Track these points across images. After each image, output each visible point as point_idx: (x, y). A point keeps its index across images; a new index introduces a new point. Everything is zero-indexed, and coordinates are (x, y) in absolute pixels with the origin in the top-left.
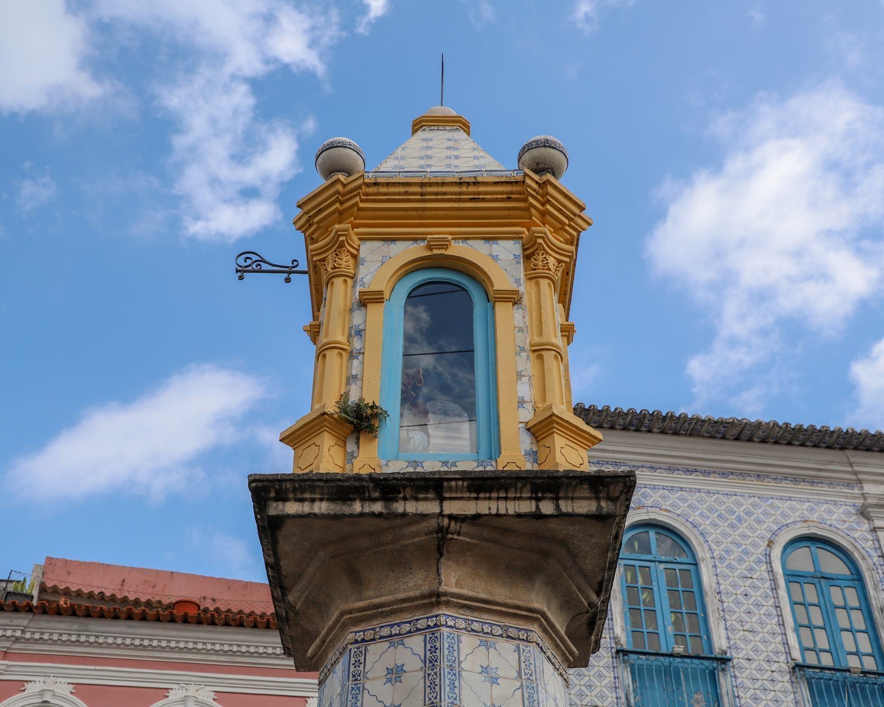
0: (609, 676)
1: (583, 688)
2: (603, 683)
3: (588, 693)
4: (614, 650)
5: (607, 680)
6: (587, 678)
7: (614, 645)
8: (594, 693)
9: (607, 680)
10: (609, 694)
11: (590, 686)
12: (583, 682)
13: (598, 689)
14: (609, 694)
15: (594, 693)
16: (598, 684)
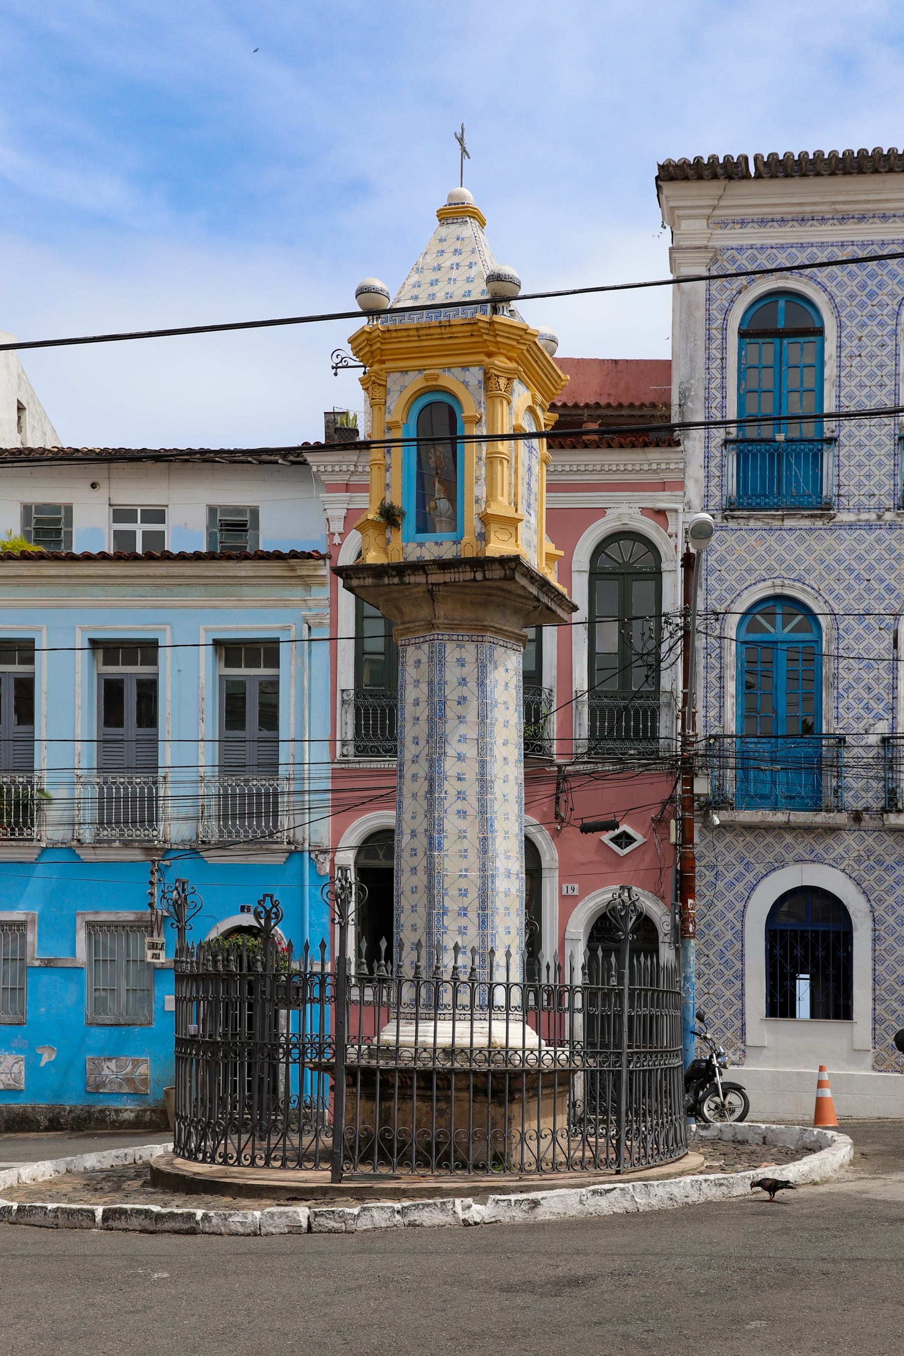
0: (889, 463)
1: (862, 478)
2: (882, 472)
3: (866, 483)
4: (897, 437)
5: (887, 468)
6: (867, 468)
7: (897, 432)
8: (872, 482)
9: (887, 468)
10: (887, 482)
11: (869, 476)
12: (862, 473)
13: (877, 478)
14: (887, 482)
15: (872, 482)
16: (877, 473)
